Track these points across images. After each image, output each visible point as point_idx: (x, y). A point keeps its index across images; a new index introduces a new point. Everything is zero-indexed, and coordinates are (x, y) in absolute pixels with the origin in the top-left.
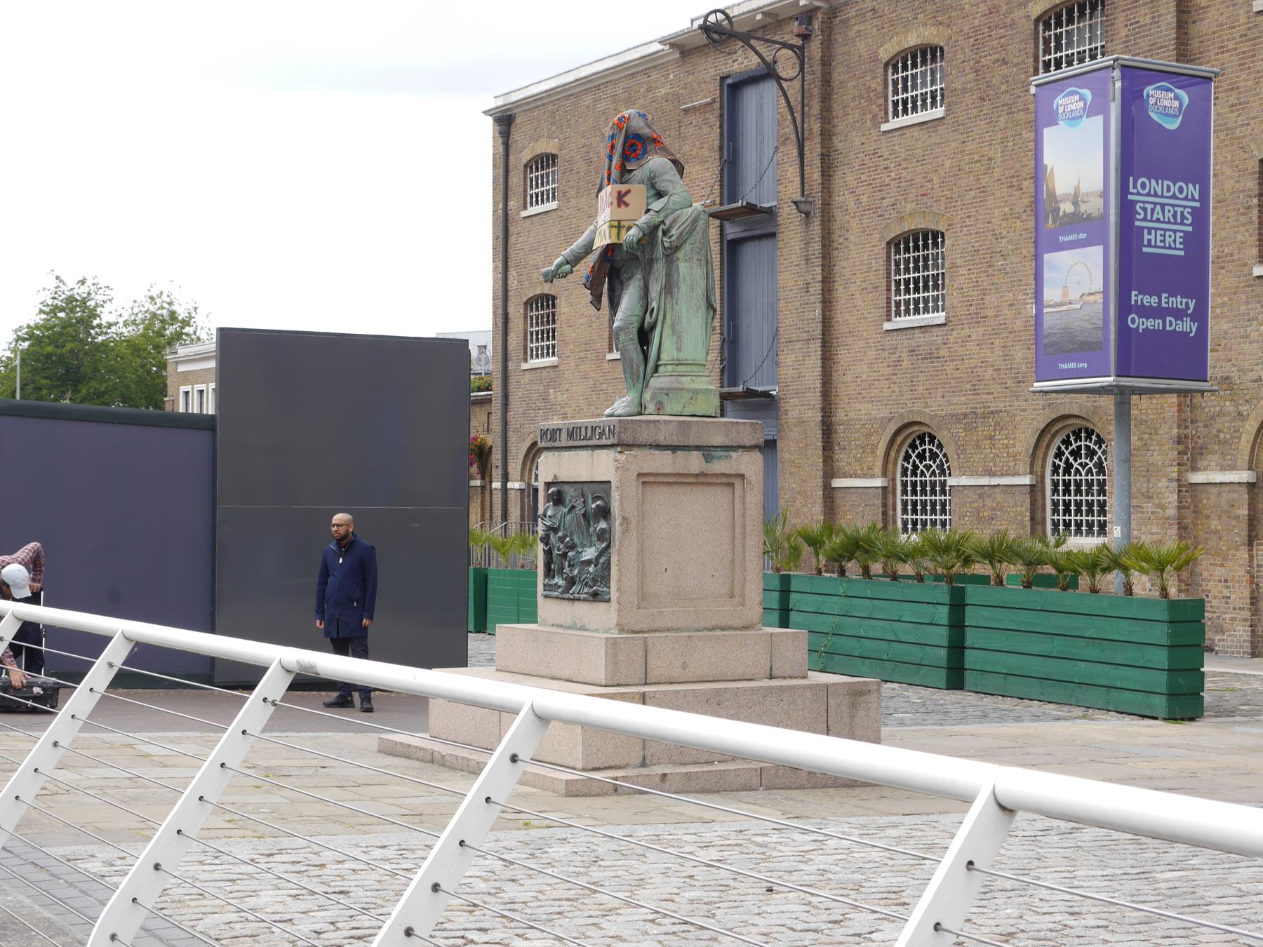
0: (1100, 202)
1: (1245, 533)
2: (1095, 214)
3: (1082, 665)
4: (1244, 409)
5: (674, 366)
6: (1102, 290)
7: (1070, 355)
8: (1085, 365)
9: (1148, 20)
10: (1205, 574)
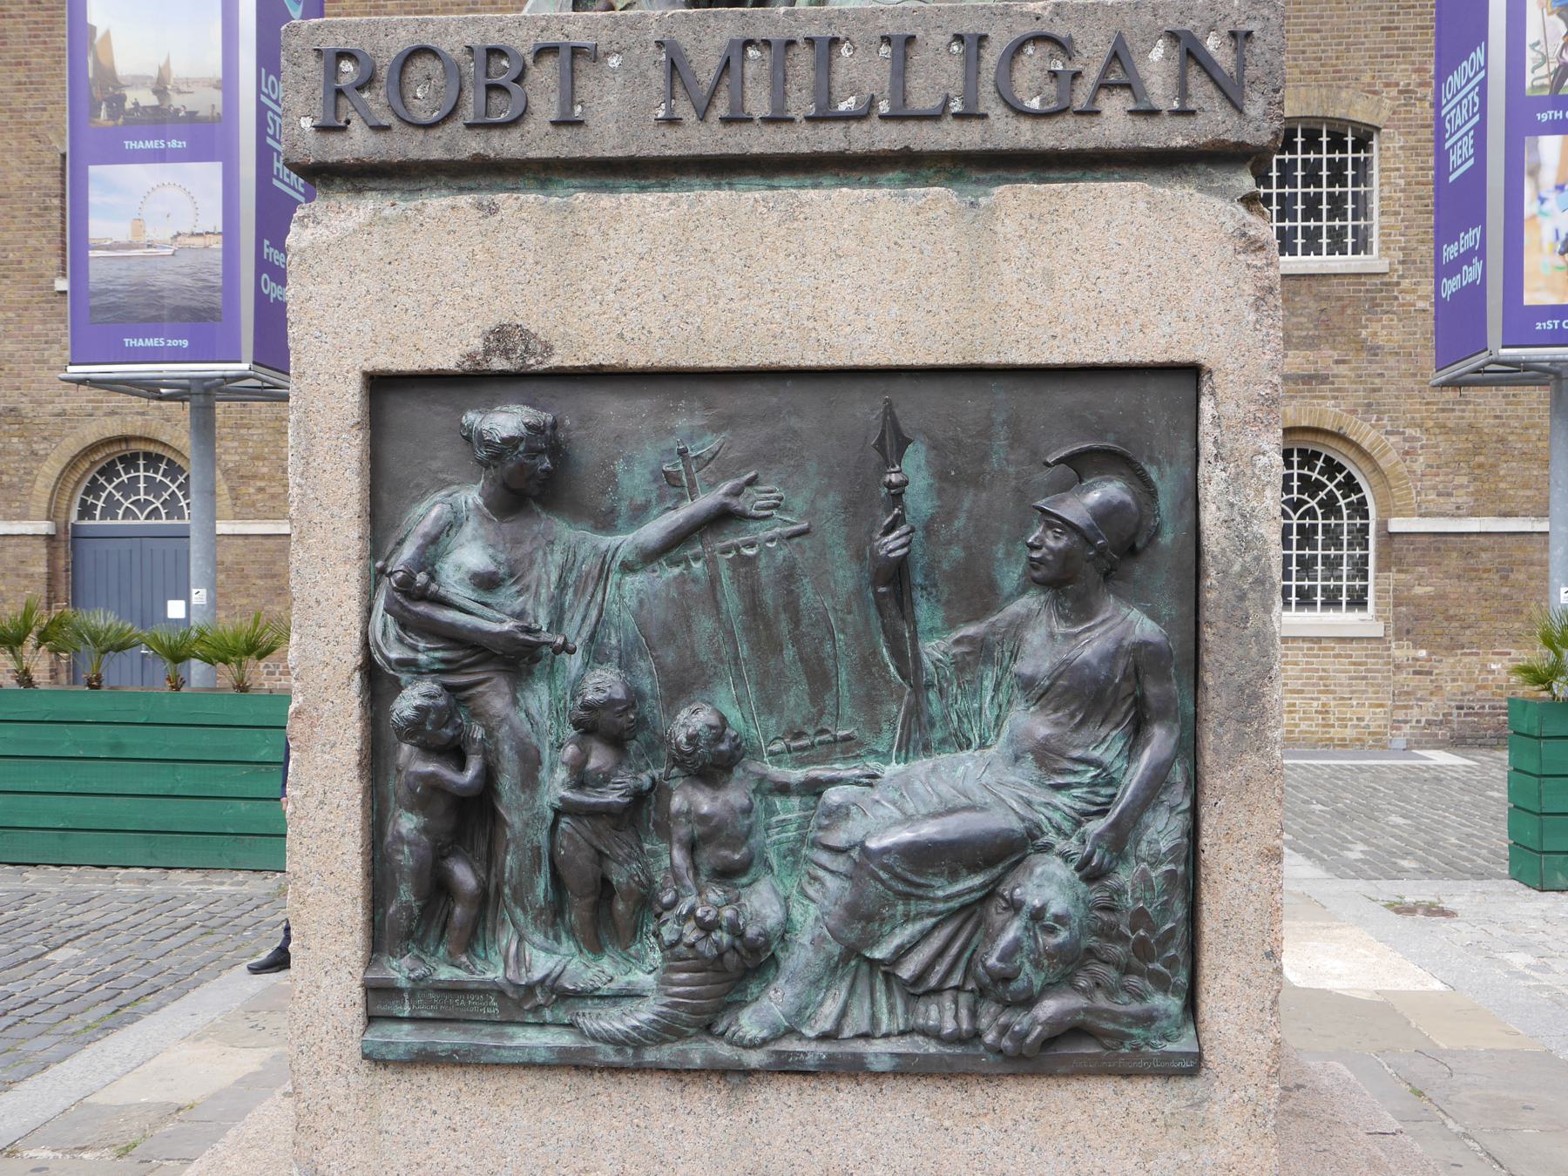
0: (217, 97)
2: (204, 112)
3: (243, 806)
4: (40, 447)
6: (220, 229)
7: (152, 325)
8: (185, 343)
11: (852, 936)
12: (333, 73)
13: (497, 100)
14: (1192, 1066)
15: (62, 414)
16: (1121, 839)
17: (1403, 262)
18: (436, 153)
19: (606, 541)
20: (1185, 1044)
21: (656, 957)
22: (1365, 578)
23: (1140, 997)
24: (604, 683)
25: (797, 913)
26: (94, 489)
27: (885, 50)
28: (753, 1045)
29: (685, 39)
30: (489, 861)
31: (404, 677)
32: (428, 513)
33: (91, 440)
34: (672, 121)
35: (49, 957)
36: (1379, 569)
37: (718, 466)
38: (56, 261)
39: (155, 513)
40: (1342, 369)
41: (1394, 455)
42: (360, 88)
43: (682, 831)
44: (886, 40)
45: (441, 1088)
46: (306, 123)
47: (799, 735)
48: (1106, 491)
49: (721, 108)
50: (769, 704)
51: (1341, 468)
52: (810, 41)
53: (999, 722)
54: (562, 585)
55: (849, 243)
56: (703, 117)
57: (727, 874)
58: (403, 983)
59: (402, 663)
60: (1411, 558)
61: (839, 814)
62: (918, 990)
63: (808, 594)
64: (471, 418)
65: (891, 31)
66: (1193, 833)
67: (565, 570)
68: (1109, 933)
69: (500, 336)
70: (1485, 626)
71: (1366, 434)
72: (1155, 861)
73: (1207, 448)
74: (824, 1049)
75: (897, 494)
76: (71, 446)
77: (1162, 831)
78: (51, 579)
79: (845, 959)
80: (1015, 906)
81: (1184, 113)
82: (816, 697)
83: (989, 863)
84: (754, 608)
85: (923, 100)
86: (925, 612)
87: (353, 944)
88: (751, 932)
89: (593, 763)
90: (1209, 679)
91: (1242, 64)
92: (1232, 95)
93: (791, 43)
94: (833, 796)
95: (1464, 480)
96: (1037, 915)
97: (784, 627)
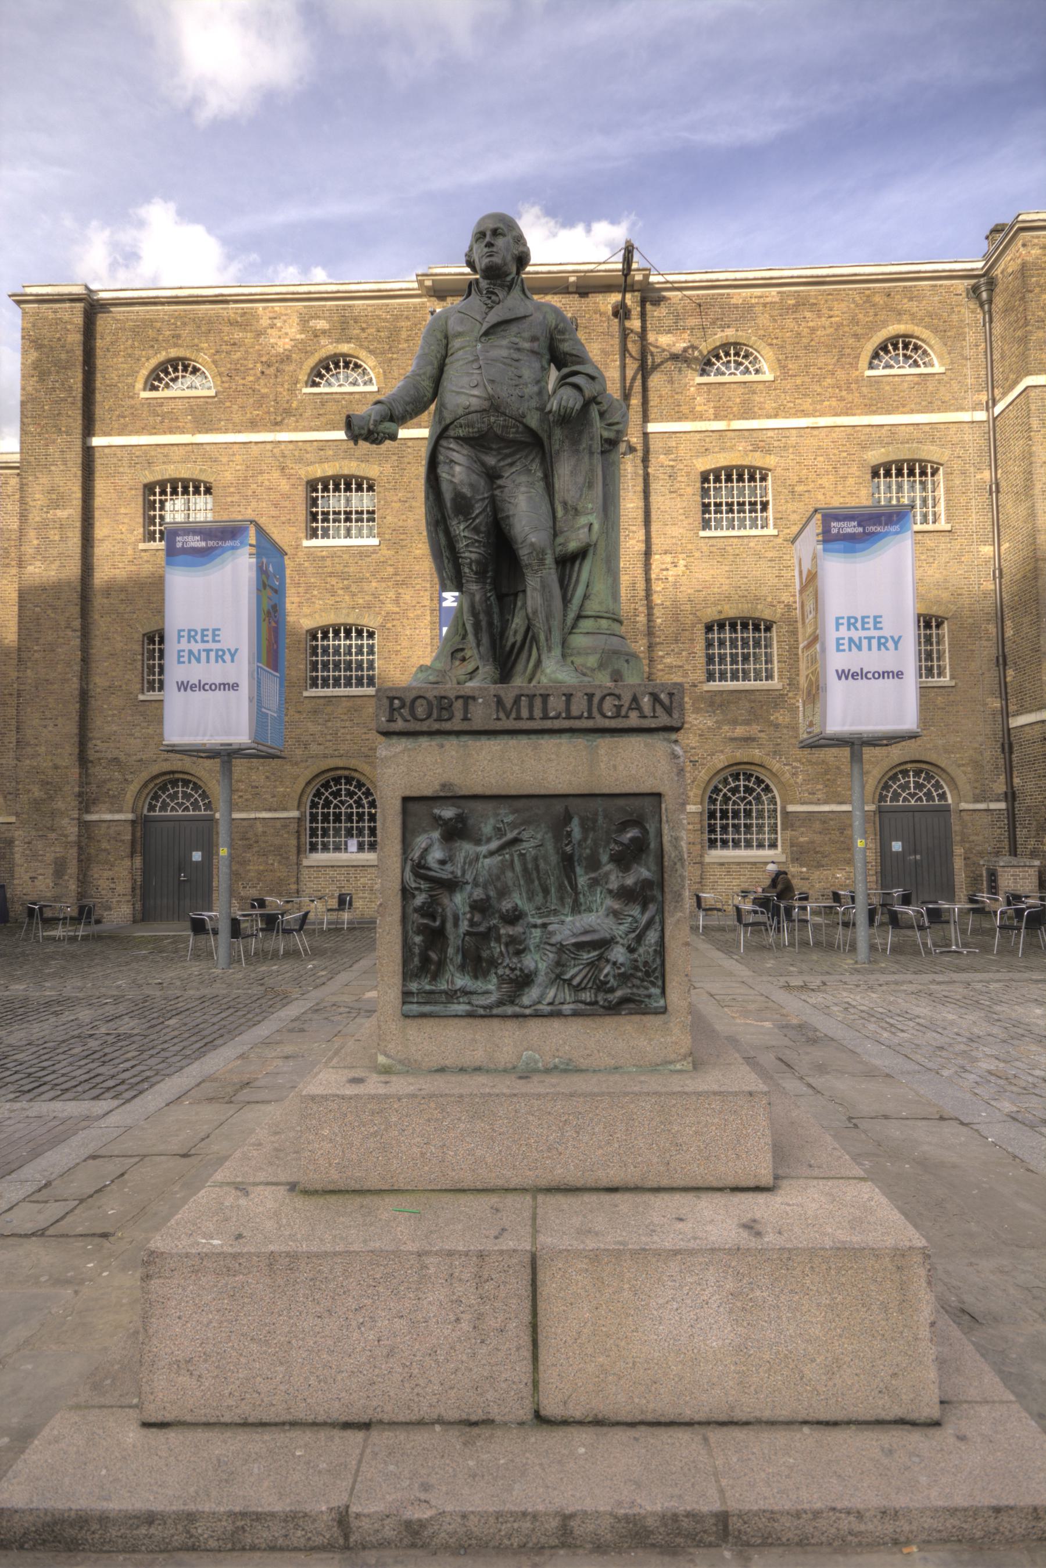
1: (128, 850)
4: (129, 777)
5: (610, 621)
9: (57, 538)
10: (96, 876)
11: (558, 971)
12: (391, 704)
13: (444, 712)
14: (664, 1011)
15: (141, 760)
16: (639, 939)
17: (789, 685)
18: (425, 729)
19: (479, 849)
20: (662, 1003)
21: (495, 980)
22: (776, 833)
23: (647, 989)
24: (478, 894)
25: (540, 965)
26: (156, 797)
27: (564, 698)
28: (526, 1007)
29: (502, 694)
30: (443, 951)
31: (416, 893)
32: (421, 841)
33: (155, 773)
34: (498, 719)
35: (167, 1023)
36: (783, 829)
37: (513, 825)
38: (139, 686)
39: (187, 809)
40: (762, 735)
41: (788, 775)
42: (400, 708)
43: (503, 940)
44: (564, 695)
45: (428, 1024)
46: (383, 719)
47: (539, 909)
48: (631, 834)
49: (513, 715)
50: (530, 899)
51: (763, 781)
52: (541, 695)
53: (602, 903)
54: (465, 863)
55: (553, 757)
56: (508, 717)
57: (518, 953)
58: (415, 990)
59: (417, 889)
60: (798, 823)
61: (552, 934)
62: (578, 989)
63: (542, 865)
64: (436, 811)
65: (565, 692)
66: (662, 937)
67: (465, 858)
68: (636, 968)
69: (443, 786)
70: (833, 857)
71: (775, 765)
72: (650, 946)
73: (664, 818)
74: (549, 1008)
75: (569, 834)
76: (145, 776)
77: (652, 937)
78: (133, 842)
79: (556, 979)
80: (608, 961)
81: (654, 717)
82: (545, 897)
83: (600, 948)
84: (525, 870)
85: (575, 712)
86: (579, 870)
87: (398, 980)
88: (526, 971)
89: (475, 919)
90: (666, 890)
91: (671, 702)
92: (669, 711)
93: (535, 695)
94: (551, 928)
95: (820, 787)
96: (615, 963)
97: (535, 875)
